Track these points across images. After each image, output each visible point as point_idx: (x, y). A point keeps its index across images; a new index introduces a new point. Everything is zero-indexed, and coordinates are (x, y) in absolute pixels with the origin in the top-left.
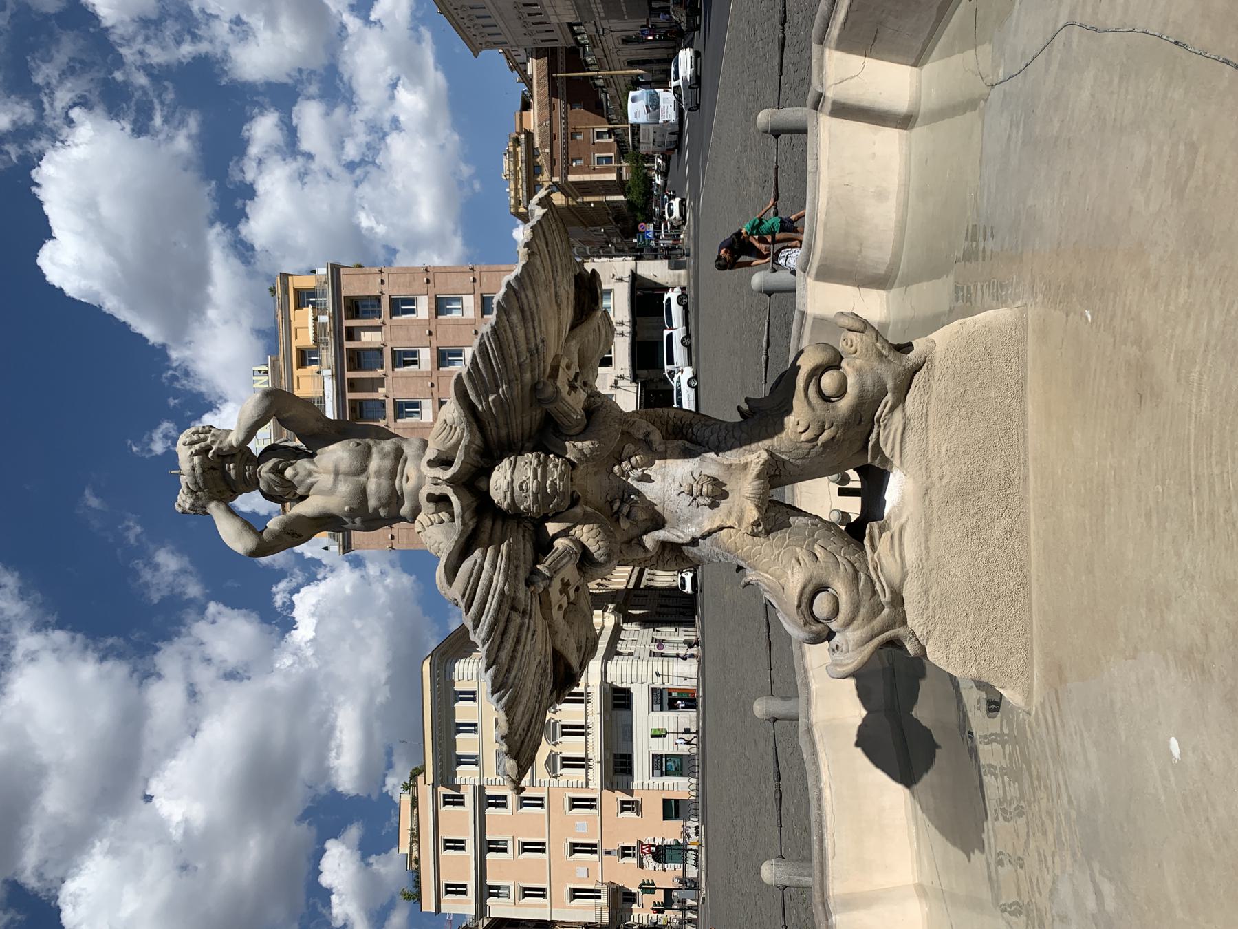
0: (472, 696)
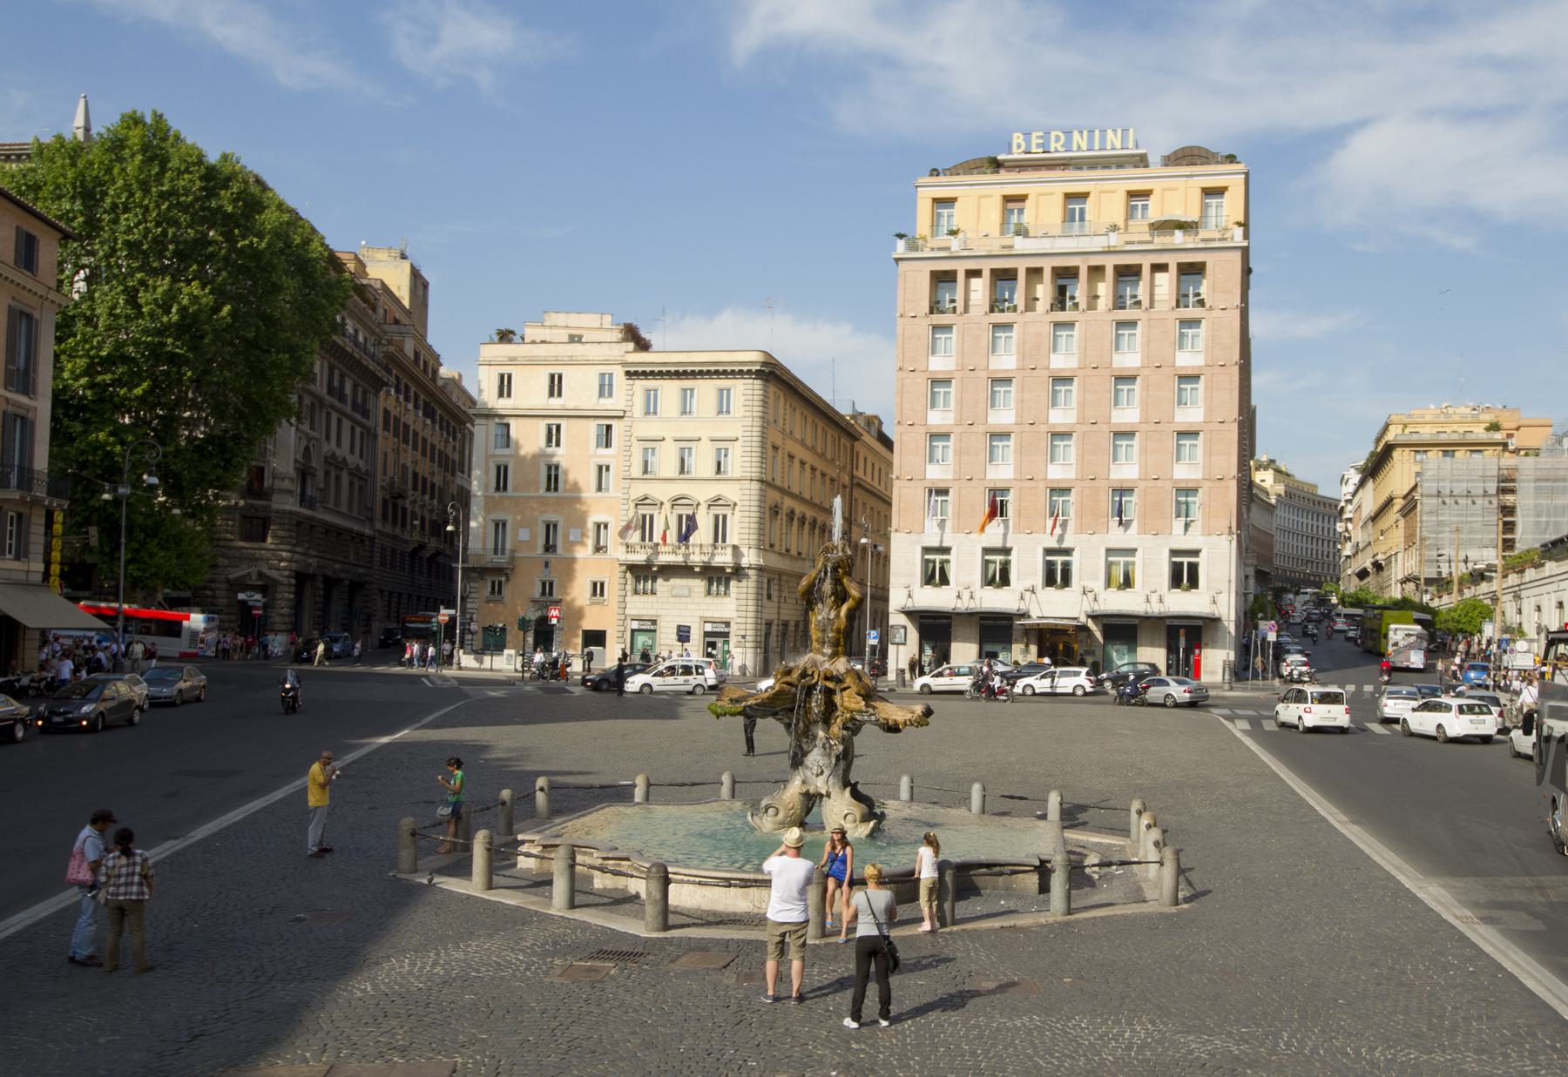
0: (725, 410)
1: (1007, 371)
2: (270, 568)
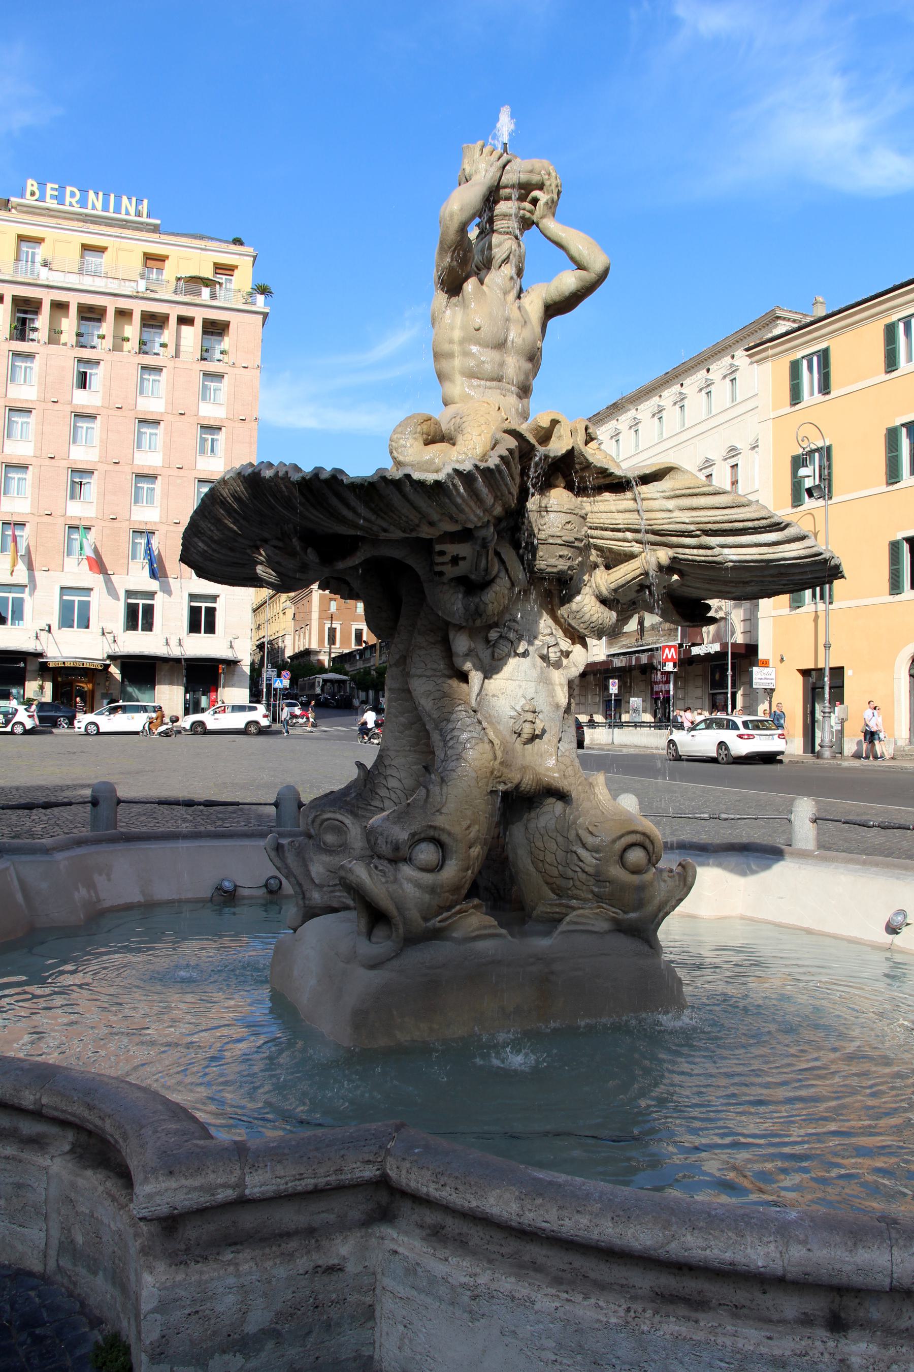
1: (27, 401)
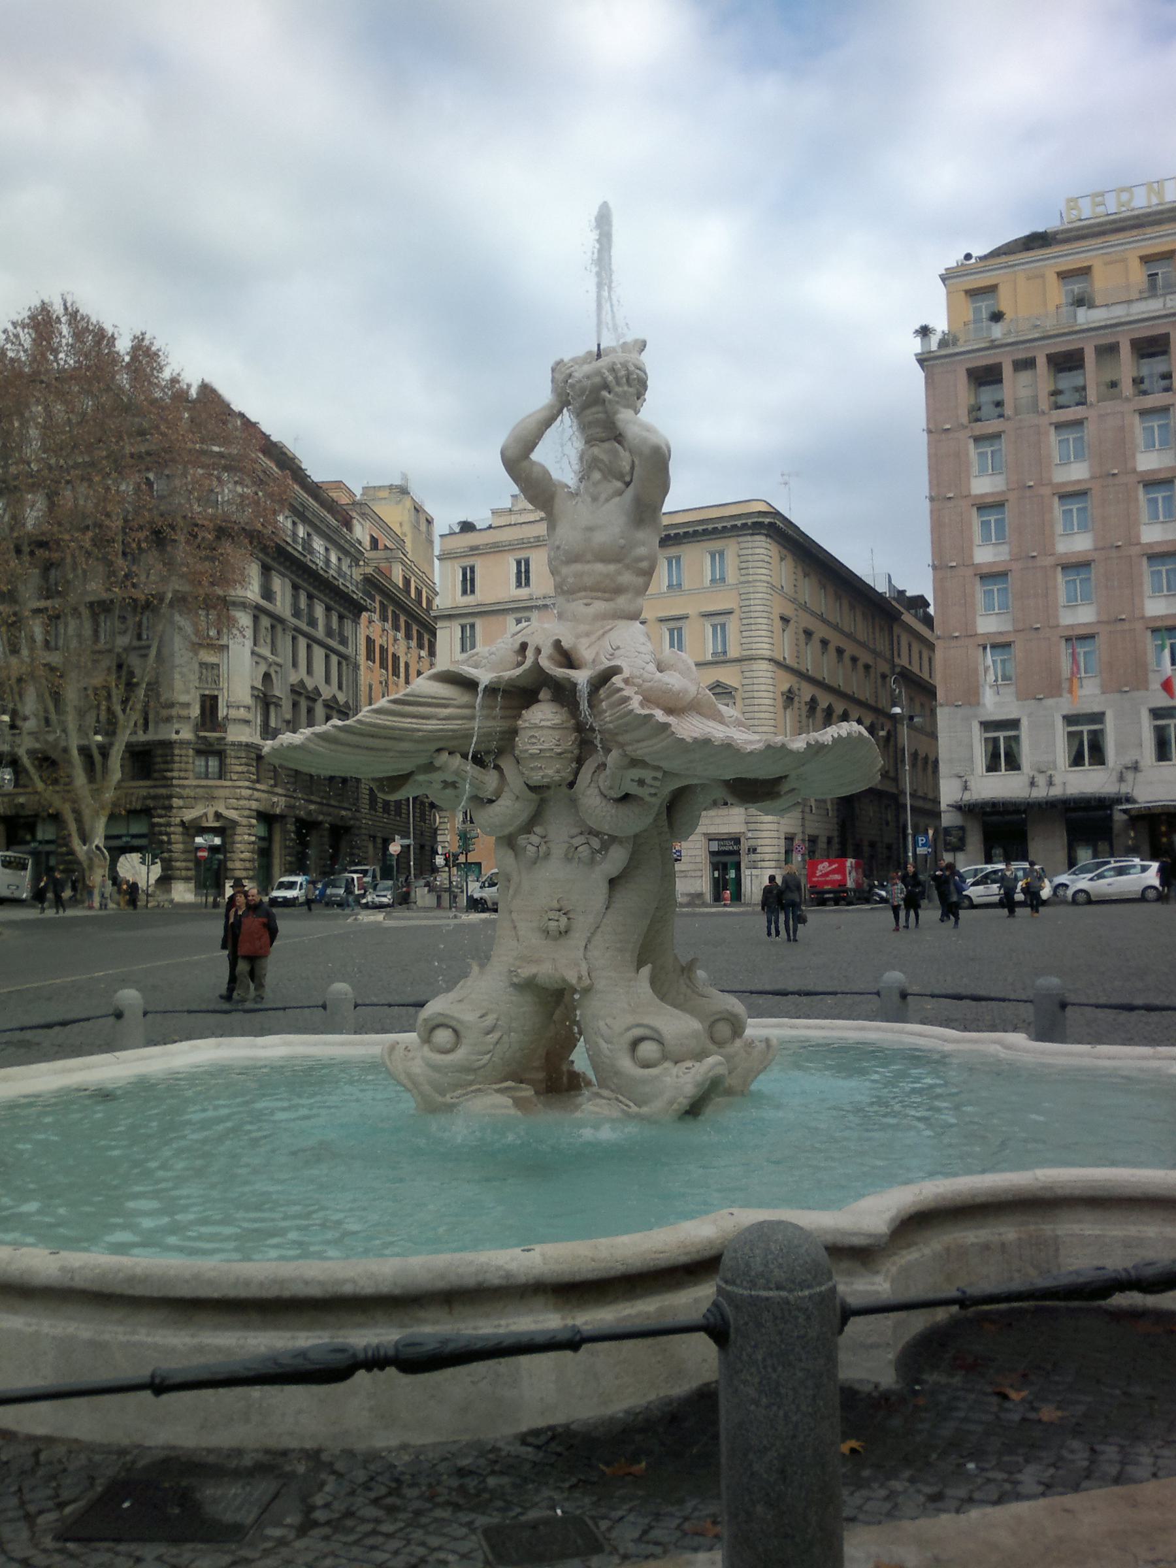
1: (1079, 482)
2: (227, 808)
